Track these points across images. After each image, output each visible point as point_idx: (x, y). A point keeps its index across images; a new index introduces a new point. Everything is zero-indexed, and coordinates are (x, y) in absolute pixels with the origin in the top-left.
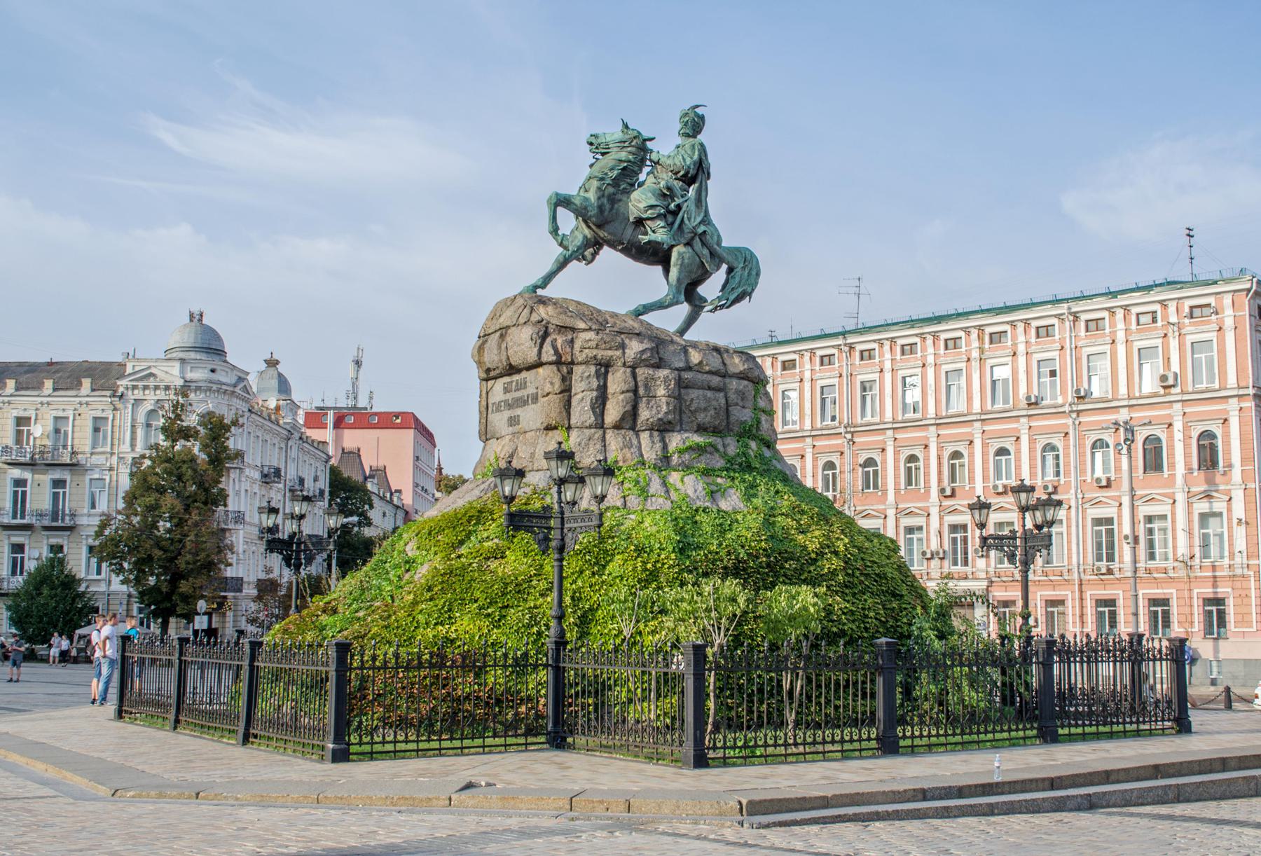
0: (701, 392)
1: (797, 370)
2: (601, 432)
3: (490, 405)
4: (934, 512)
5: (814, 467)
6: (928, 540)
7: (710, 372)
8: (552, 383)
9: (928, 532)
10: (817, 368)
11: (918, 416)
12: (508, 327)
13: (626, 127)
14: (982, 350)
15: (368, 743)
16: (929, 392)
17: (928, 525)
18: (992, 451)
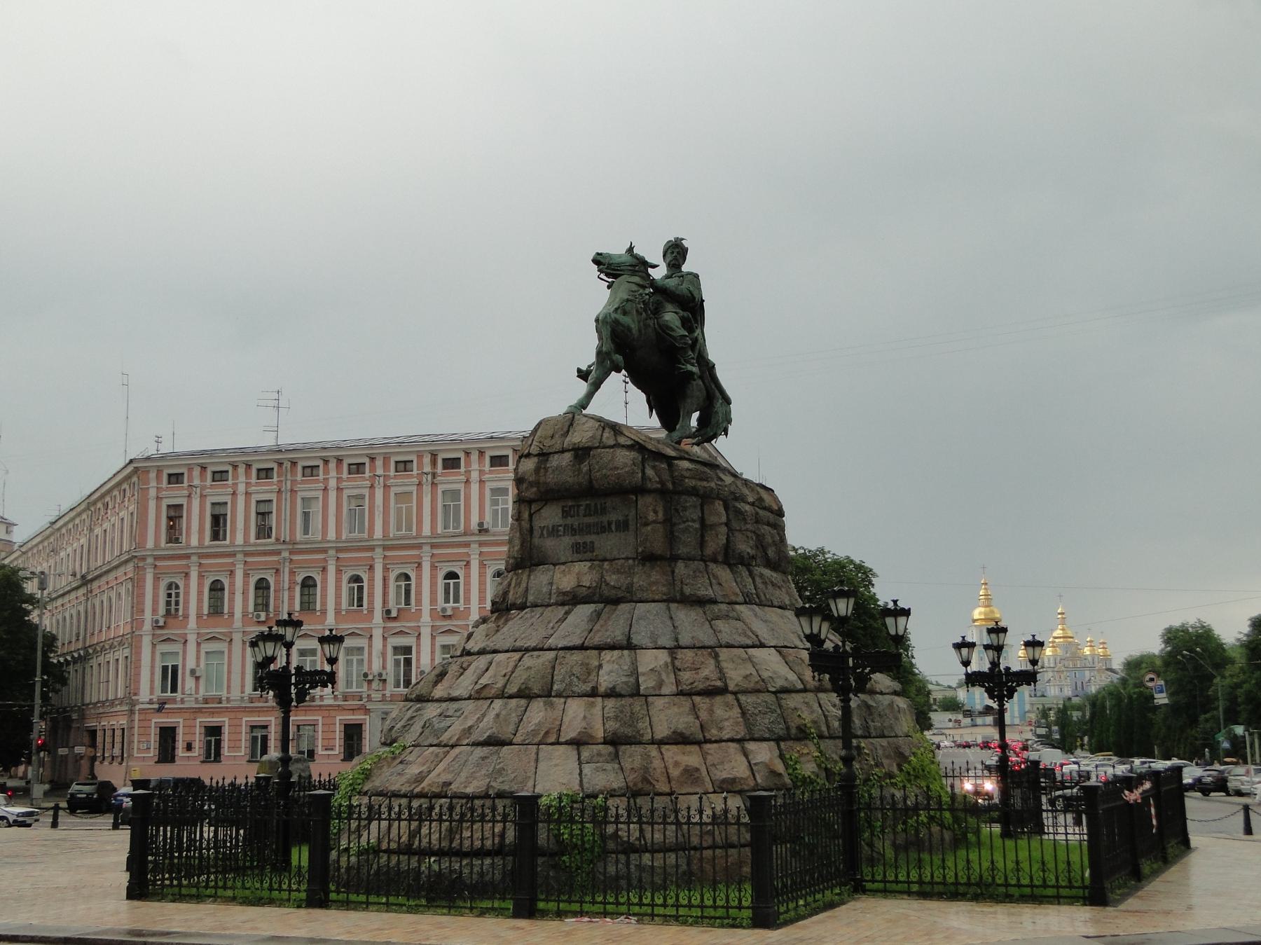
0: (766, 527)
1: (230, 482)
2: (701, 563)
3: (536, 528)
4: (377, 634)
5: (246, 584)
6: (370, 661)
7: (765, 508)
8: (656, 512)
9: (370, 654)
10: (254, 480)
11: (366, 535)
12: (589, 449)
13: (631, 249)
14: (434, 475)
15: (601, 903)
16: (377, 513)
17: (370, 646)
18: (441, 575)
